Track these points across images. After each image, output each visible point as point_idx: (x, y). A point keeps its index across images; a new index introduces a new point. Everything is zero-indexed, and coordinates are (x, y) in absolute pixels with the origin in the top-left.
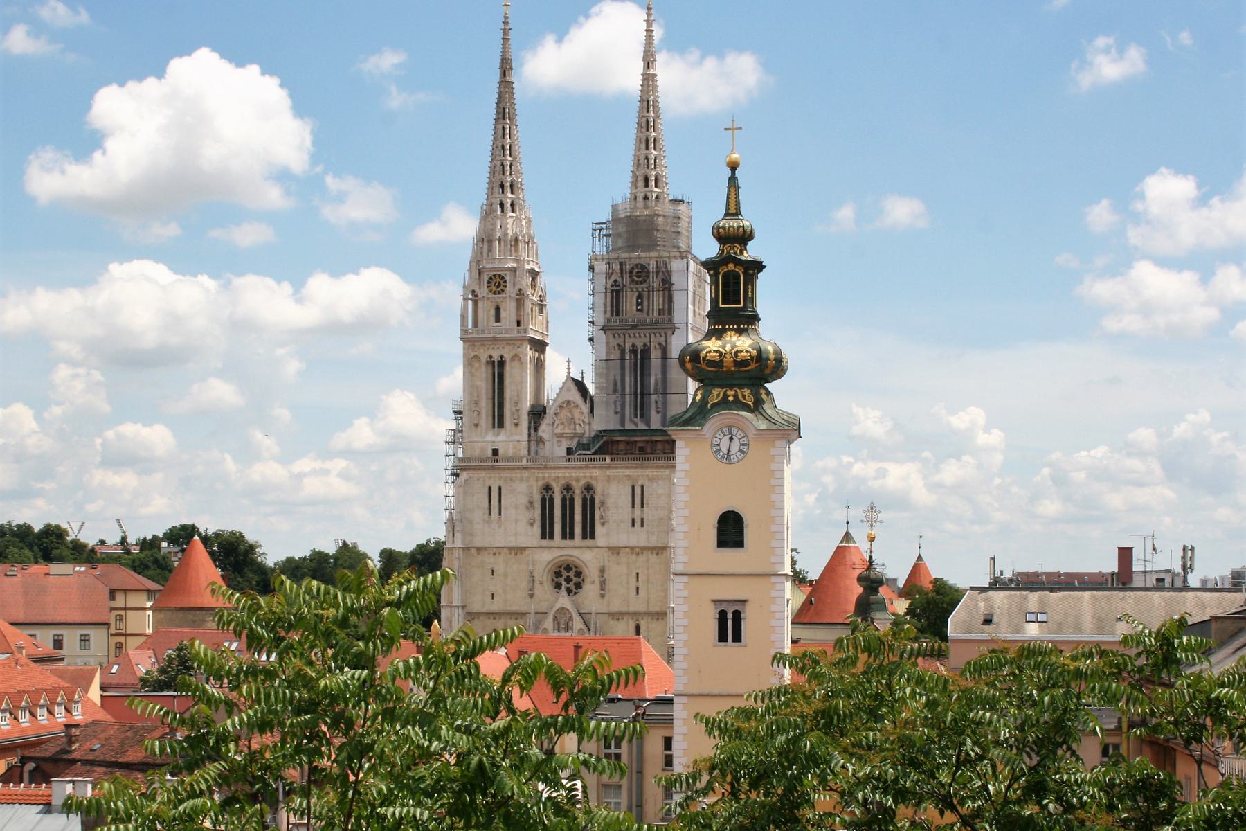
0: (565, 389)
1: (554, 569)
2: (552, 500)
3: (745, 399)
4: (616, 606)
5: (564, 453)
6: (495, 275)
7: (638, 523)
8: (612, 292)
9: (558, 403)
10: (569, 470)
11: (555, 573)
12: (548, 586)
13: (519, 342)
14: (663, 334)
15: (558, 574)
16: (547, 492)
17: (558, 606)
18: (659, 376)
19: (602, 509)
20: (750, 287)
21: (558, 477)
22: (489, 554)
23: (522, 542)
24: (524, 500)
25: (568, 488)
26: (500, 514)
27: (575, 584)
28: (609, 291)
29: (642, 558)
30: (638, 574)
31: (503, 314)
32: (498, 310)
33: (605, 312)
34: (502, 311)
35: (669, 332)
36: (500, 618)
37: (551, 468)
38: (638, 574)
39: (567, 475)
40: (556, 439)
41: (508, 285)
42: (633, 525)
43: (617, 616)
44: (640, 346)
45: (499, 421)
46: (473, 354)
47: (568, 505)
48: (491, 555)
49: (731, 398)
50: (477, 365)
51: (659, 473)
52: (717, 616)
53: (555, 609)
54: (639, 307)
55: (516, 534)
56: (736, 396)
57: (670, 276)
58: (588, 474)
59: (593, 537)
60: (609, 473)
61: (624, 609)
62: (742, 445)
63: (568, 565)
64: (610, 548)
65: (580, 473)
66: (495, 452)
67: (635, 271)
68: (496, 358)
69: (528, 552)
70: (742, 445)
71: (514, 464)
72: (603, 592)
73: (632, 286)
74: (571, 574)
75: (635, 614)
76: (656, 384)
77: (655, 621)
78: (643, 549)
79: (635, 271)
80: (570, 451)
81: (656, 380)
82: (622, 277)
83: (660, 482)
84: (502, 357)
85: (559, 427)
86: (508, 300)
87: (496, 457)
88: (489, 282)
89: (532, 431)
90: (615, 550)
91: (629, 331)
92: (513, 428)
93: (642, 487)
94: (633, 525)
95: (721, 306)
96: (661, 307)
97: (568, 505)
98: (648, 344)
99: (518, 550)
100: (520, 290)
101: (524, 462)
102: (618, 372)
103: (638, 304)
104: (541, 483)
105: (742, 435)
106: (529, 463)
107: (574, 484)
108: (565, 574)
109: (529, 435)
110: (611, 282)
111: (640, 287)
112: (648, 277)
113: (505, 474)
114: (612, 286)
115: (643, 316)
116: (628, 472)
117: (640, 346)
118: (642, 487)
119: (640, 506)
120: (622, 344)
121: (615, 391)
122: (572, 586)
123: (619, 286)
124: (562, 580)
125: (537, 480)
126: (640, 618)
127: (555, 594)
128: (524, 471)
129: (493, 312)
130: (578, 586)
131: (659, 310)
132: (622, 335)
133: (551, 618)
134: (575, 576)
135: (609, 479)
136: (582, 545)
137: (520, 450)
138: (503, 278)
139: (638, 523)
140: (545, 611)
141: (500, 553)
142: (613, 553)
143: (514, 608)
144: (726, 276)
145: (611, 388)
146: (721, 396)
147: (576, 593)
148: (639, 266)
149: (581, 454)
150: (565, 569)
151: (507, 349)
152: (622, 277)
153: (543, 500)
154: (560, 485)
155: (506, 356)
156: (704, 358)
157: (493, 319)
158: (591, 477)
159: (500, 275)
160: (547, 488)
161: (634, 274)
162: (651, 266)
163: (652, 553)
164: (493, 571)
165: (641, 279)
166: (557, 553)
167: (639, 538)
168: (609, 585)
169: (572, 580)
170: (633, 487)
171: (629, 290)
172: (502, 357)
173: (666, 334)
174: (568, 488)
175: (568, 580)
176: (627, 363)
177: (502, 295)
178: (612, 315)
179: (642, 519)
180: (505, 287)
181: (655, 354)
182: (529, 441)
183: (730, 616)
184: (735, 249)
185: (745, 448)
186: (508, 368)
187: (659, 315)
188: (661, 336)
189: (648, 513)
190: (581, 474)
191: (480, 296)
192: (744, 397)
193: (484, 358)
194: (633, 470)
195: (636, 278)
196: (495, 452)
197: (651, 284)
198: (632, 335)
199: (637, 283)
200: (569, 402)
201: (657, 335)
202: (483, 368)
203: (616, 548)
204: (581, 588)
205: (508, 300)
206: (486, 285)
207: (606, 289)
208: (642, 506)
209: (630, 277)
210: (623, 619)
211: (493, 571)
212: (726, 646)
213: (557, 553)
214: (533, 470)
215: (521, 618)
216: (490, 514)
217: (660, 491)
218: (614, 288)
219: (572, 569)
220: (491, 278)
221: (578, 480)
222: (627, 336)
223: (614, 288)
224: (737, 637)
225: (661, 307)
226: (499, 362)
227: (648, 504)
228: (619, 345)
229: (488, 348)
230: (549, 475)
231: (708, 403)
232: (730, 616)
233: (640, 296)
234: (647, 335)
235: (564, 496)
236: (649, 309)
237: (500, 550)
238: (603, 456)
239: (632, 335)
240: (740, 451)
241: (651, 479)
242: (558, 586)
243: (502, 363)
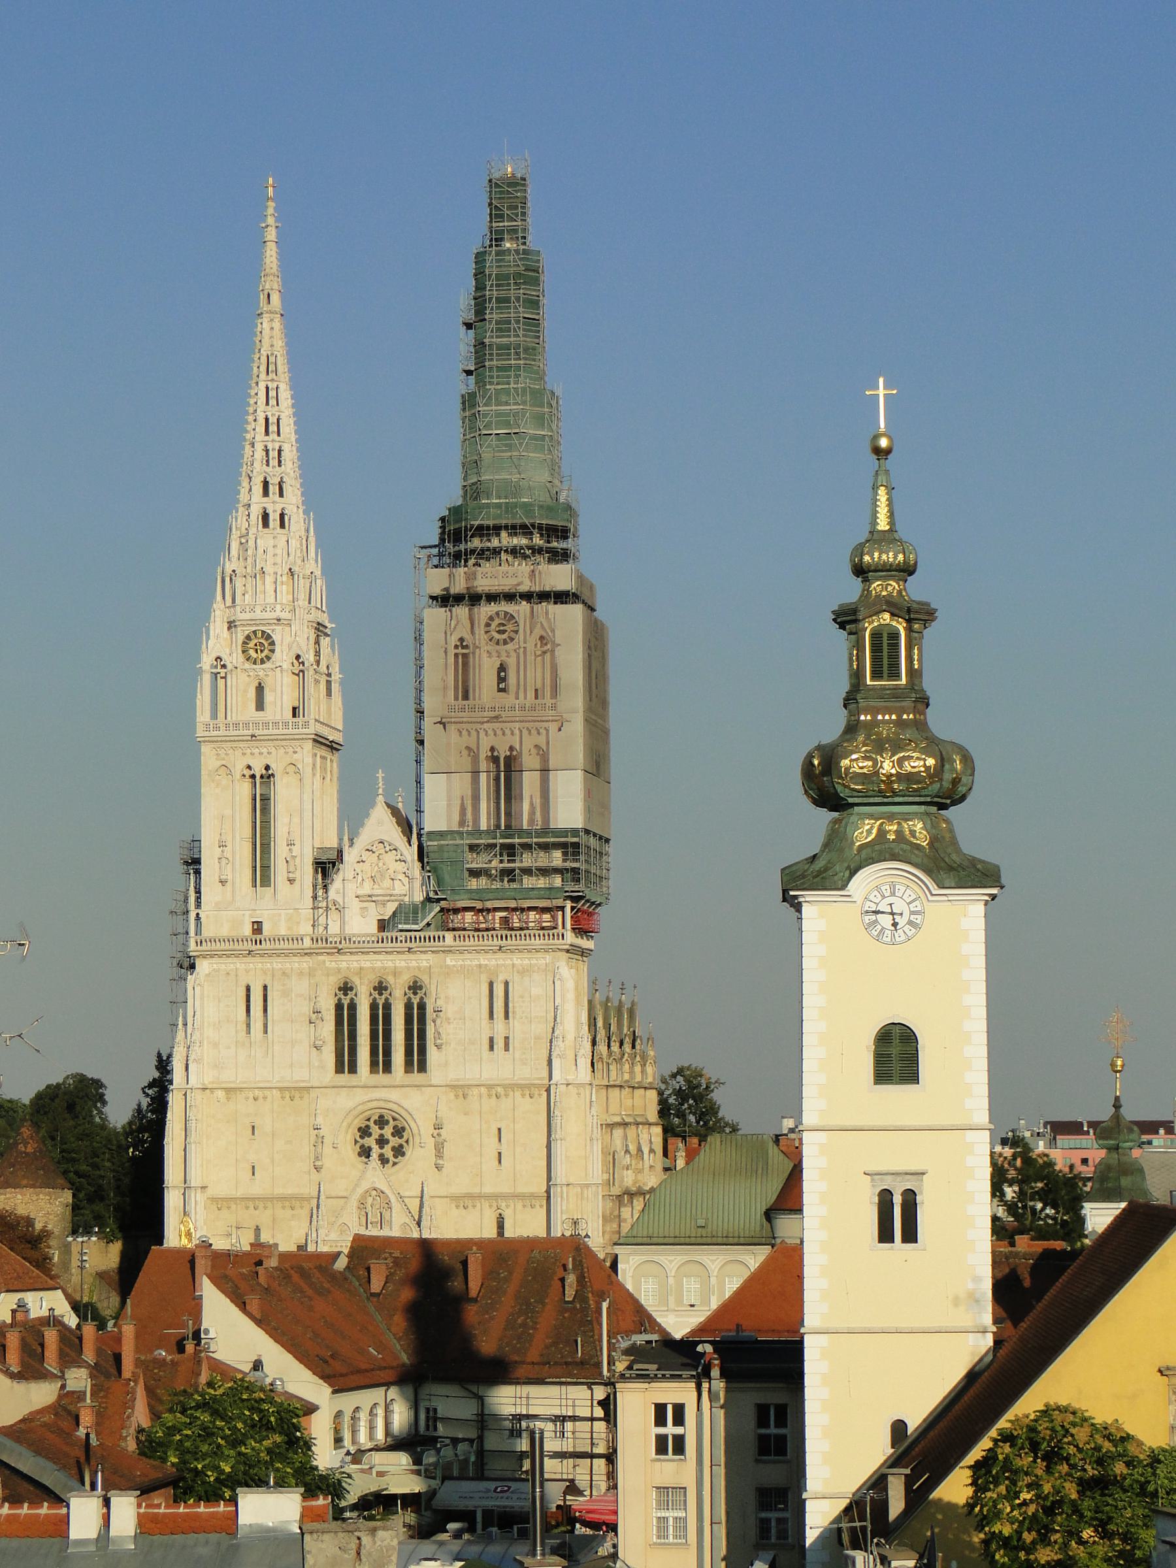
1: (359, 1122)
2: (353, 1007)
3: (914, 837)
4: (462, 1185)
5: (374, 929)
6: (255, 632)
7: (499, 1044)
8: (456, 655)
10: (381, 957)
11: (360, 1129)
12: (350, 1152)
13: (297, 743)
14: (543, 731)
15: (365, 1132)
16: (346, 994)
17: (365, 1185)
18: (537, 801)
19: (438, 1022)
20: (916, 651)
21: (361, 968)
22: (247, 1098)
23: (300, 1076)
24: (306, 1009)
25: (381, 988)
26: (266, 1032)
27: (393, 1149)
28: (451, 660)
29: (506, 1103)
30: (499, 1129)
31: (269, 697)
32: (260, 689)
33: (445, 688)
34: (267, 692)
35: (553, 727)
36: (265, 1208)
38: (499, 1129)
41: (278, 648)
42: (491, 1048)
43: (464, 1201)
44: (503, 753)
45: (262, 874)
46: (219, 763)
47: (381, 1017)
48: (251, 1099)
49: (892, 837)
50: (225, 781)
51: (534, 962)
52: (876, 1200)
53: (360, 1191)
54: (502, 686)
55: (291, 1066)
56: (899, 833)
57: (553, 631)
58: (414, 964)
59: (422, 1068)
60: (450, 960)
61: (476, 1190)
62: (912, 913)
63: (381, 1117)
64: (453, 1087)
65: (400, 962)
66: (257, 927)
67: (497, 621)
68: (258, 770)
69: (314, 1093)
70: (912, 913)
71: (290, 946)
72: (441, 1162)
73: (490, 648)
74: (388, 1131)
75: (496, 1197)
76: (532, 813)
77: (529, 1209)
78: (511, 1087)
79: (497, 621)
80: (383, 925)
81: (532, 804)
82: (473, 632)
83: (536, 976)
84: (267, 768)
87: (258, 937)
89: (320, 893)
90: (461, 1090)
91: (486, 726)
93: (506, 984)
94: (491, 1048)
95: (869, 682)
96: (539, 685)
97: (381, 1017)
98: (518, 747)
99: (295, 1092)
102: (470, 793)
103: (501, 680)
104: (334, 981)
105: (876, 893)
106: (315, 946)
107: (390, 979)
108: (375, 1131)
109: (315, 897)
110: (453, 640)
111: (501, 647)
112: (516, 632)
113: (277, 964)
114: (456, 647)
115: (508, 699)
116: (483, 960)
117: (503, 753)
118: (506, 984)
119: (502, 1015)
120: (474, 747)
121: (462, 823)
122: (388, 1152)
123: (467, 647)
124: (370, 1142)
125: (328, 975)
126: (504, 1204)
127: (361, 1166)
130: (399, 1151)
131: (536, 690)
132: (474, 733)
133: (354, 1203)
134: (393, 1135)
135: (448, 972)
136: (372, 1084)
138: (269, 637)
139: (499, 1044)
140: (344, 1194)
141: (265, 1098)
142: (457, 1096)
143: (290, 1191)
144: (876, 635)
145: (456, 817)
146: (875, 831)
147: (395, 1164)
148: (502, 615)
149: (401, 931)
150: (375, 1123)
152: (473, 632)
153: (339, 1007)
154: (366, 982)
155: (272, 766)
156: (847, 769)
157: (253, 705)
158: (419, 968)
159: (263, 632)
160: (346, 988)
161: (494, 625)
162: (522, 615)
163: (523, 1096)
164: (253, 1127)
165: (505, 636)
166: (360, 1096)
167: (498, 1068)
168: (447, 1150)
169: (387, 1142)
170: (491, 984)
171: (485, 655)
172: (267, 768)
173: (547, 730)
174: (381, 988)
175: (382, 1142)
176: (483, 777)
177: (268, 665)
178: (456, 698)
179: (507, 1038)
180: (273, 651)
181: (529, 760)
183: (897, 1200)
184: (890, 588)
185: (917, 919)
187: (536, 698)
188: (539, 733)
189: (517, 1027)
190: (403, 964)
191: (229, 666)
192: (913, 833)
193: (239, 767)
194: (489, 956)
195: (497, 636)
196: (257, 927)
197: (522, 645)
198: (490, 732)
199: (498, 643)
201: (534, 732)
203: (462, 1086)
204: (403, 1154)
207: (446, 652)
208: (507, 1017)
209: (487, 632)
210: (474, 1206)
211: (253, 1127)
212: (892, 1249)
213: (360, 1096)
214: (321, 958)
215: (302, 1207)
216: (249, 1032)
217: (535, 991)
218: (460, 651)
219: (387, 1122)
220: (248, 638)
221: (395, 973)
222: (482, 734)
223: (460, 651)
224: (910, 1235)
225: (539, 685)
227: (514, 1012)
228: (468, 748)
230: (348, 964)
231: (853, 843)
232: (897, 1200)
233: (502, 668)
234: (517, 732)
235: (375, 999)
236: (518, 688)
237: (267, 1093)
238: (441, 933)
239: (490, 732)
240: (910, 923)
241: (524, 972)
242: (365, 1152)
243: (268, 776)
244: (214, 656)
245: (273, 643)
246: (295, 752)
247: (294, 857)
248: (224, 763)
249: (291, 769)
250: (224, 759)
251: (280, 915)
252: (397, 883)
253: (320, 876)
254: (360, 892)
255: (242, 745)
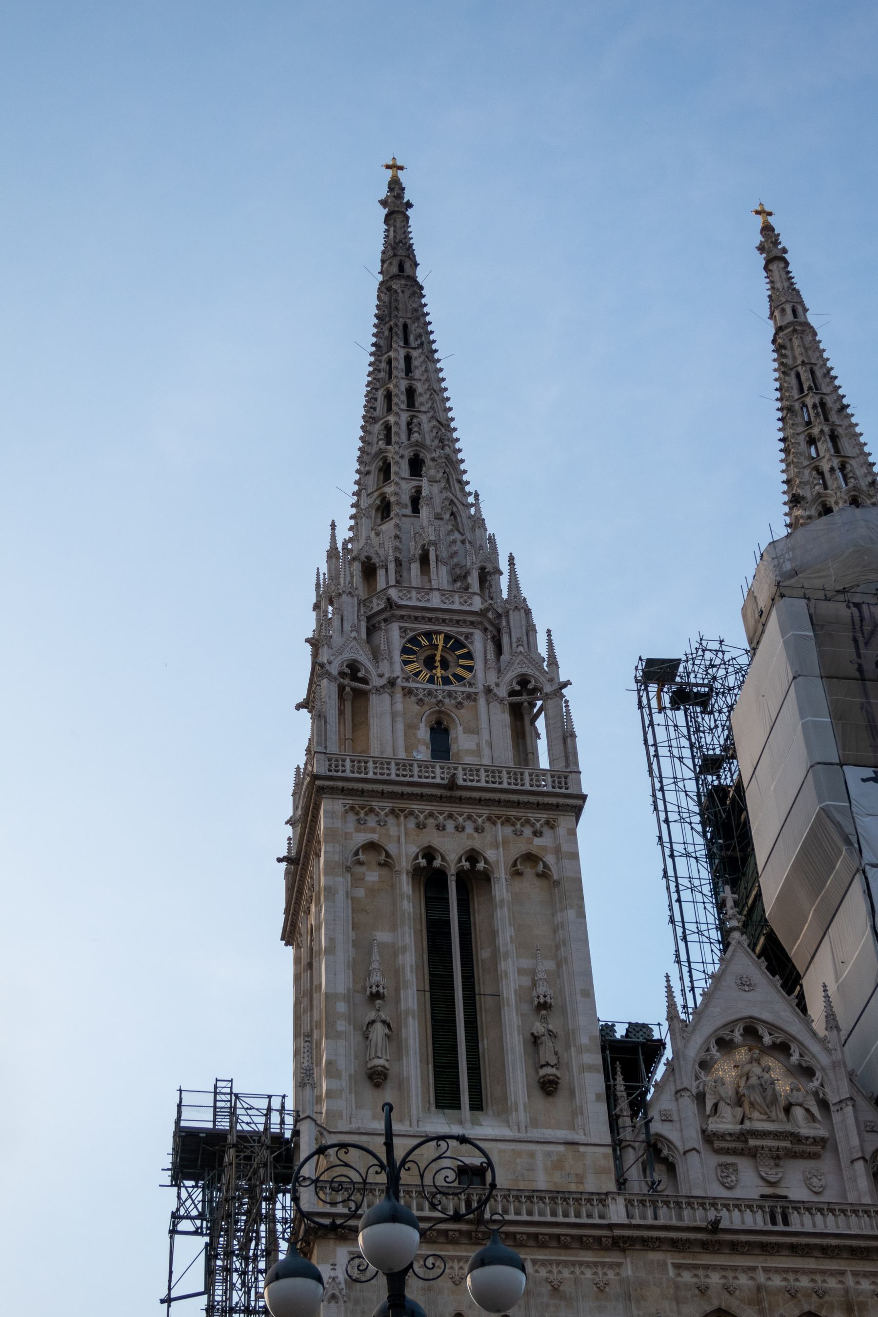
0: (730, 981)
6: (428, 635)
9: (707, 1028)
13: (543, 816)
37: (735, 1248)
39: (804, 1282)
40: (713, 1160)
41: (479, 664)
46: (362, 838)
50: (373, 876)
84: (473, 856)
85: (726, 1111)
86: (482, 701)
88: (405, 651)
92: (540, 1101)
100: (523, 681)
101: (617, 1212)
128: (612, 1258)
129: (423, 733)
137: (580, 1179)
151: (502, 831)
155: (490, 854)
172: (473, 856)
182: (618, 1146)
186: (501, 889)
191: (376, 682)
200: (751, 1030)
202: (405, 885)
205: (482, 701)
206: (397, 657)
207: (860, 669)
214: (654, 1256)
220: (414, 640)
226: (461, 877)
229: (421, 826)
244: (347, 656)
245: (469, 656)
246: (537, 834)
247: (551, 1034)
248: (375, 837)
249: (529, 871)
250: (373, 831)
251: (532, 1155)
252: (798, 1113)
253: (620, 1078)
254: (715, 1125)
255: (415, 806)
